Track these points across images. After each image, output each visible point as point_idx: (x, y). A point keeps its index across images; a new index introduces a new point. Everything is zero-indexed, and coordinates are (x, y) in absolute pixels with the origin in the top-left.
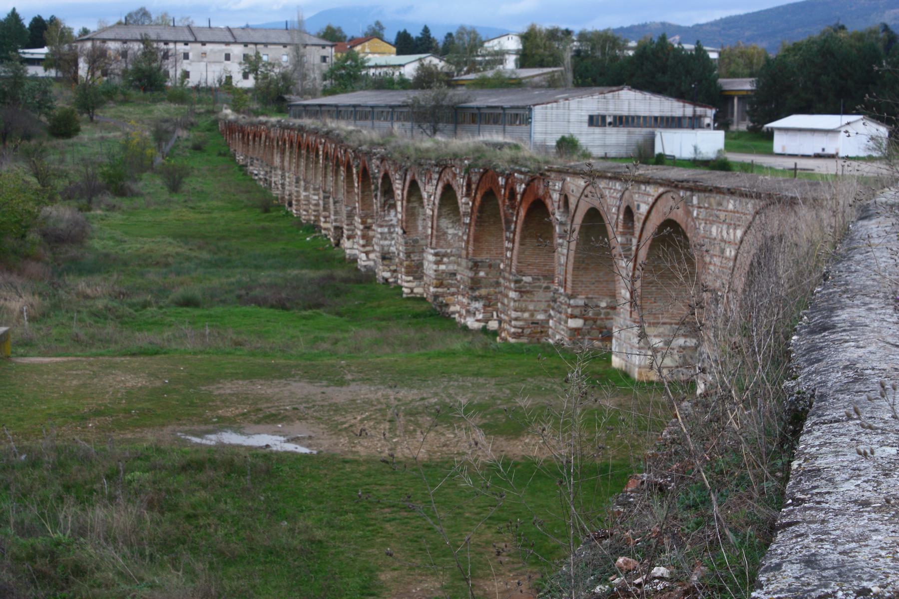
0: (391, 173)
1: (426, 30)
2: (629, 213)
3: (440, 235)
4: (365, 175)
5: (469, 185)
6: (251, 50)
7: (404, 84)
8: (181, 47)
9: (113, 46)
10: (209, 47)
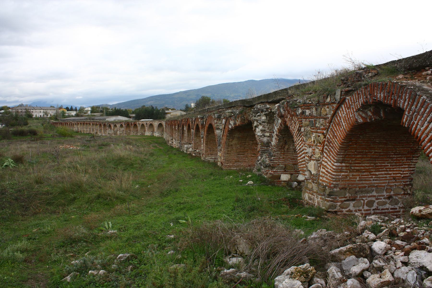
0: (111, 124)
1: (72, 107)
2: (147, 124)
3: (120, 129)
4: (105, 125)
5: (125, 124)
6: (45, 111)
7: (72, 116)
8: (32, 110)
9: (20, 110)
10: (37, 110)
